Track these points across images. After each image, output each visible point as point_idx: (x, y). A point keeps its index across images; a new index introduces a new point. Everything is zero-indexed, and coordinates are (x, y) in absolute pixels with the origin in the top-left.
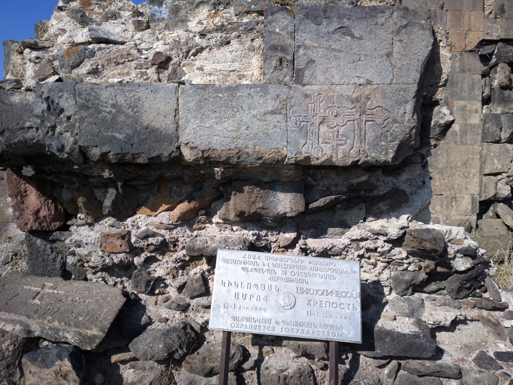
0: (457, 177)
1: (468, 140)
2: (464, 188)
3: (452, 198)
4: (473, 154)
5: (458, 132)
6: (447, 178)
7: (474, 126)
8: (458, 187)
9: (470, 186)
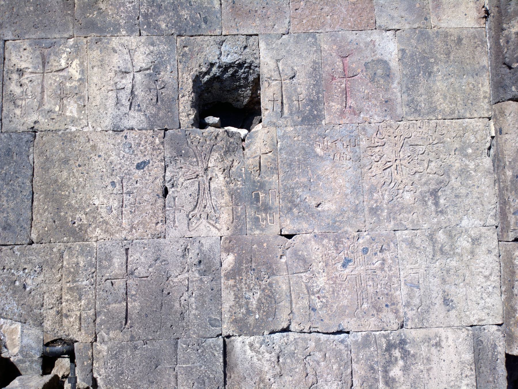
0: (403, 250)
1: (438, 97)
2: (439, 301)
3: (390, 347)
4: (462, 151)
5: (394, 64)
6: (360, 257)
8: (410, 296)
9: (462, 290)
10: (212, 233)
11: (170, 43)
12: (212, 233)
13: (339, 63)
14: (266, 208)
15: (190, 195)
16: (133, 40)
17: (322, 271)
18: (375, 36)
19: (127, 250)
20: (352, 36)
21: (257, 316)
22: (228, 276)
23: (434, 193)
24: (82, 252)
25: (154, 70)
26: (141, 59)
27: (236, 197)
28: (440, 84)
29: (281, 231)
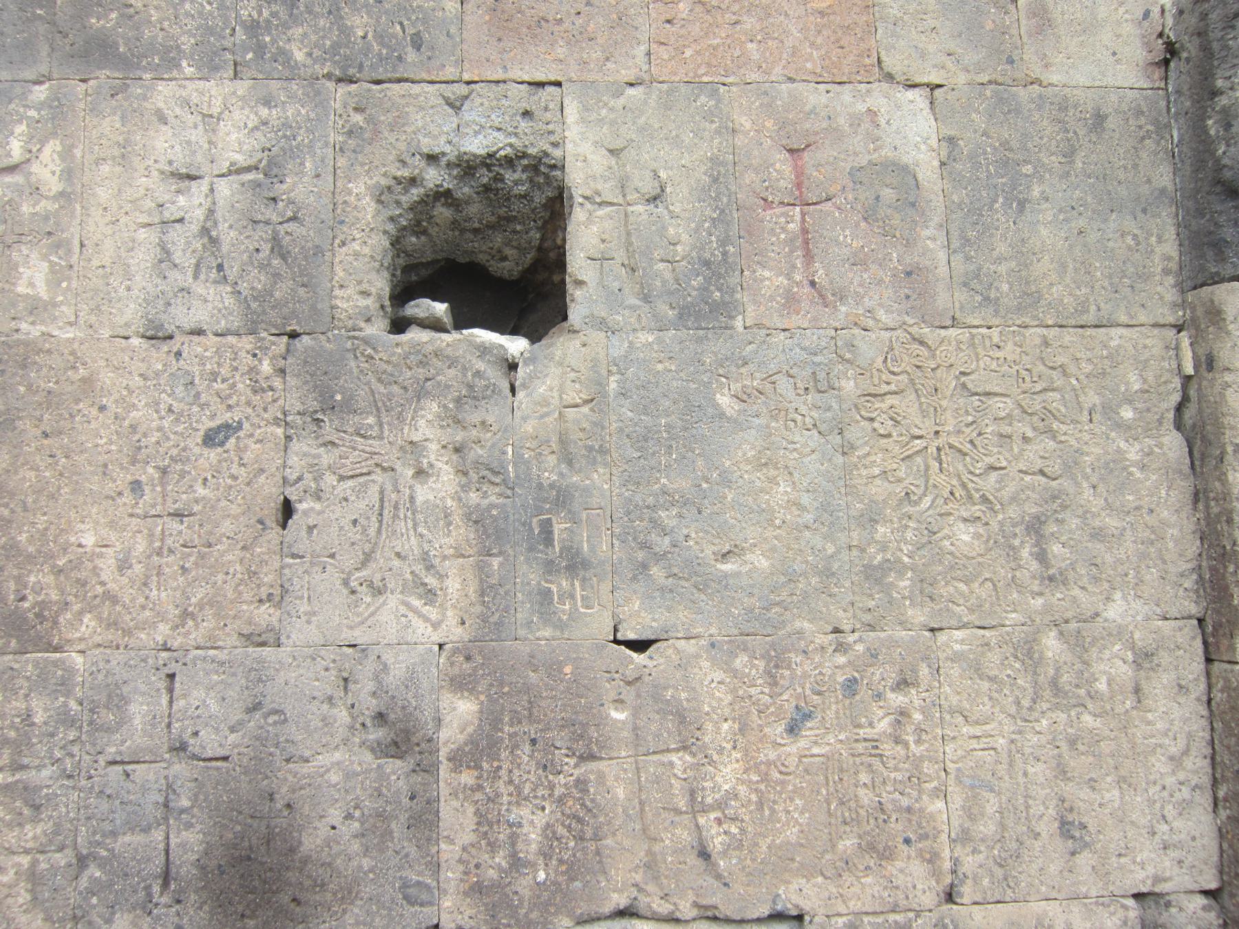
0: (953, 687)
1: (1043, 266)
2: (1047, 828)
7: (1099, 119)
8: (971, 813)
10: (414, 632)
11: (318, 100)
12: (414, 632)
13: (783, 166)
14: (575, 564)
15: (355, 522)
16: (215, 92)
17: (729, 746)
18: (879, 98)
19: (172, 676)
20: (815, 97)
21: (542, 876)
22: (458, 760)
23: (1035, 527)
24: (41, 681)
25: (267, 172)
26: (237, 142)
27: (489, 532)
28: (1047, 232)
29: (616, 630)
